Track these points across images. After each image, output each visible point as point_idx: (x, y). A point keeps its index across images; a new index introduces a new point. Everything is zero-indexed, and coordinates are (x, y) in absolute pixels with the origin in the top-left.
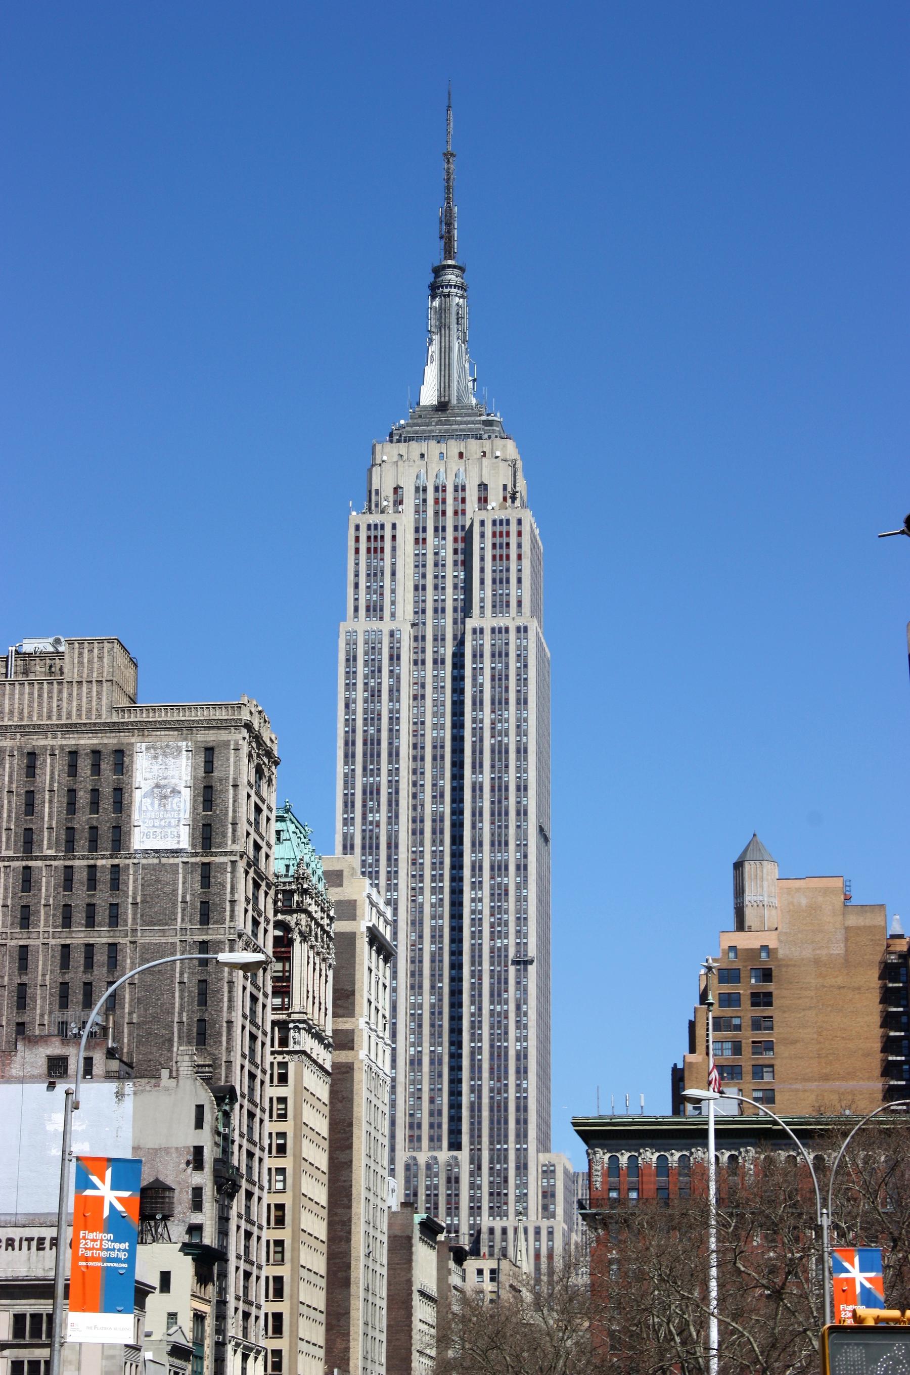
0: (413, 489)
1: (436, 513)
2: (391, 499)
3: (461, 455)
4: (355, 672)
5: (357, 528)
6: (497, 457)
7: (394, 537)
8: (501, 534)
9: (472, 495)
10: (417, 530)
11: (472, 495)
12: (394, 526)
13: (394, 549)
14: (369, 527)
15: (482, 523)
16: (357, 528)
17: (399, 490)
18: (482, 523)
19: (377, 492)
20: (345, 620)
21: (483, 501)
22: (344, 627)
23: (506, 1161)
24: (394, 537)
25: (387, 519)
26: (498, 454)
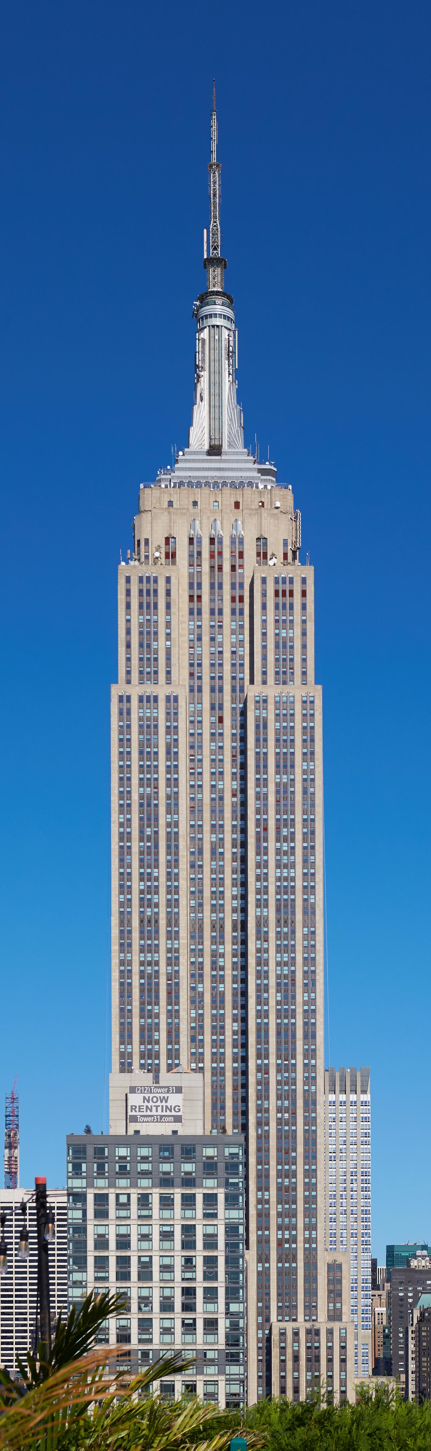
0: (186, 541)
1: (212, 567)
2: (163, 550)
3: (237, 505)
4: (129, 740)
5: (128, 580)
6: (277, 508)
7: (168, 593)
8: (284, 592)
9: (250, 551)
10: (191, 586)
11: (250, 551)
12: (168, 580)
13: (168, 606)
14: (141, 579)
15: (264, 581)
16: (128, 580)
17: (171, 540)
18: (264, 581)
19: (147, 541)
20: (116, 682)
21: (263, 556)
22: (116, 691)
23: (295, 1259)
24: (168, 593)
25: (161, 571)
26: (278, 504)
